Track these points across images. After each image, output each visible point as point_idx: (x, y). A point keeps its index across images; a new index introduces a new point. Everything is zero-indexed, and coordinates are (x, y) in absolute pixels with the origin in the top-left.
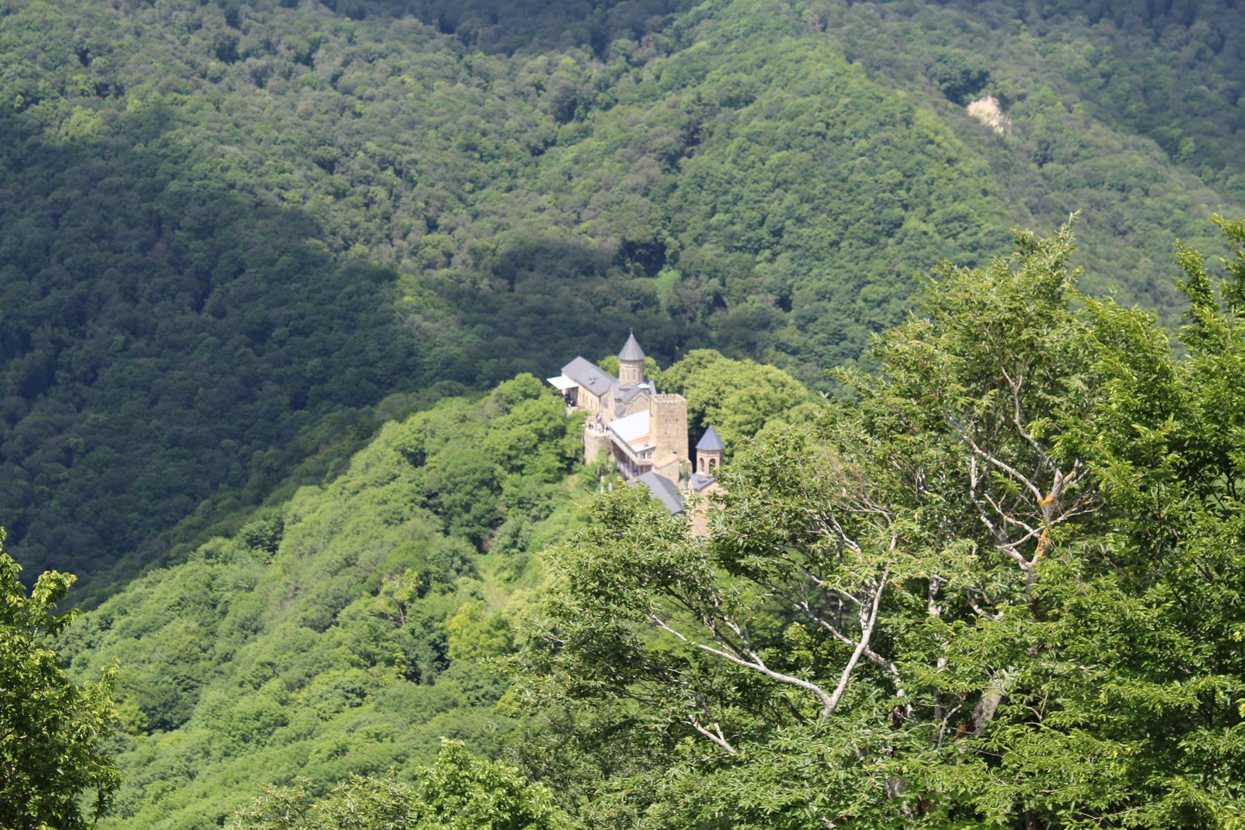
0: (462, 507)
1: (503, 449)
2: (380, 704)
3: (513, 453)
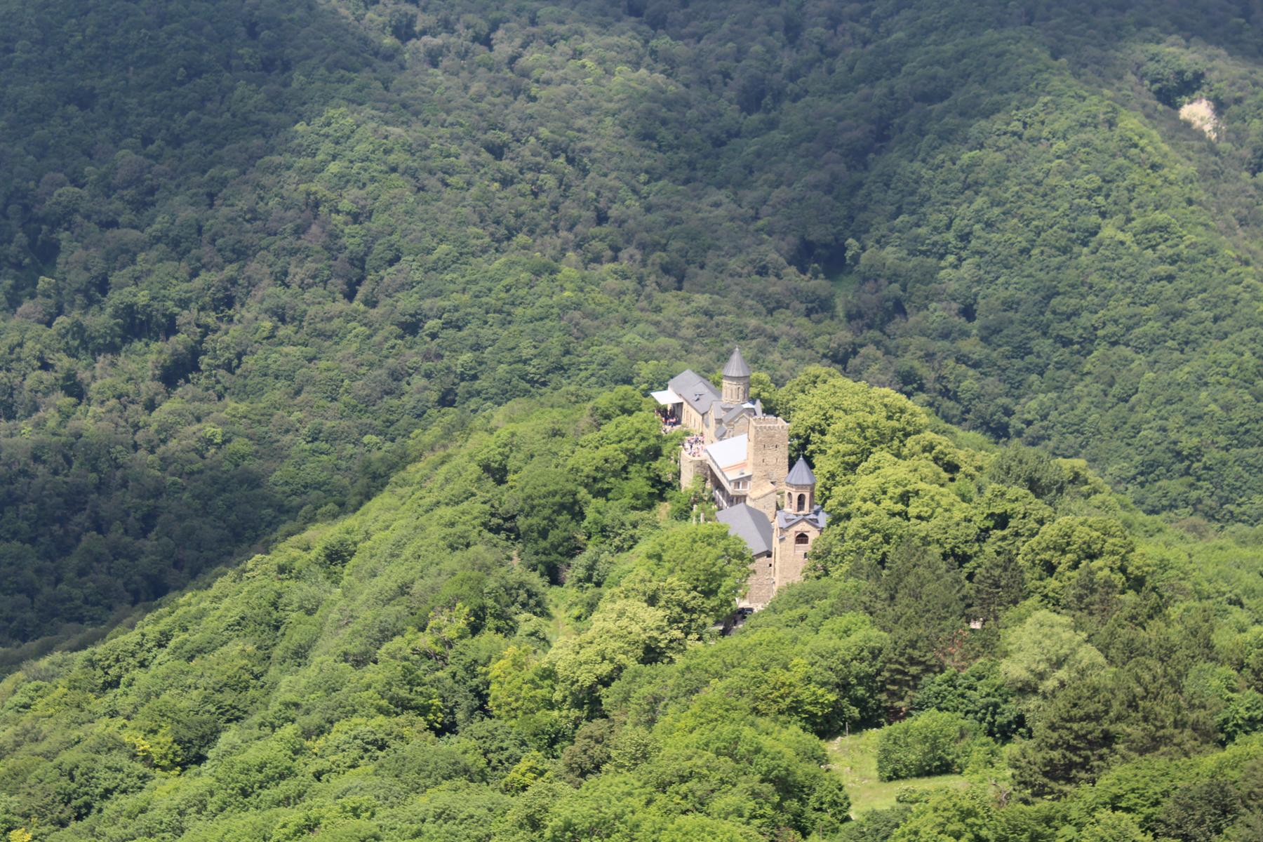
0: (539, 532)
1: (587, 470)
2: (382, 766)
3: (600, 475)
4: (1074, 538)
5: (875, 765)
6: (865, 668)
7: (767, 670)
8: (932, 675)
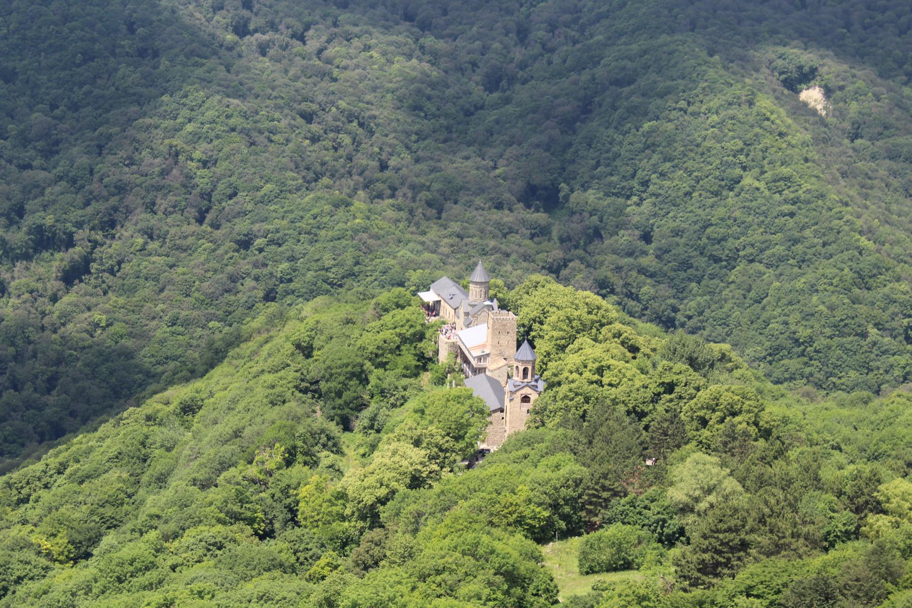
0: (336, 393)
1: (371, 348)
2: (220, 561)
3: (380, 352)
4: (721, 401)
5: (577, 563)
6: (570, 492)
7: (499, 494)
8: (618, 498)
